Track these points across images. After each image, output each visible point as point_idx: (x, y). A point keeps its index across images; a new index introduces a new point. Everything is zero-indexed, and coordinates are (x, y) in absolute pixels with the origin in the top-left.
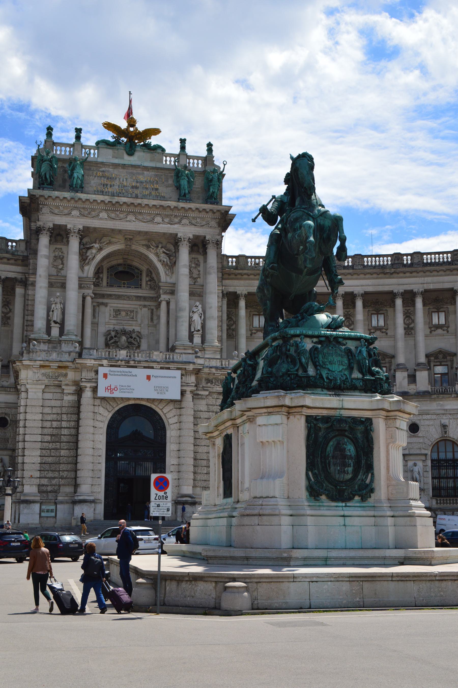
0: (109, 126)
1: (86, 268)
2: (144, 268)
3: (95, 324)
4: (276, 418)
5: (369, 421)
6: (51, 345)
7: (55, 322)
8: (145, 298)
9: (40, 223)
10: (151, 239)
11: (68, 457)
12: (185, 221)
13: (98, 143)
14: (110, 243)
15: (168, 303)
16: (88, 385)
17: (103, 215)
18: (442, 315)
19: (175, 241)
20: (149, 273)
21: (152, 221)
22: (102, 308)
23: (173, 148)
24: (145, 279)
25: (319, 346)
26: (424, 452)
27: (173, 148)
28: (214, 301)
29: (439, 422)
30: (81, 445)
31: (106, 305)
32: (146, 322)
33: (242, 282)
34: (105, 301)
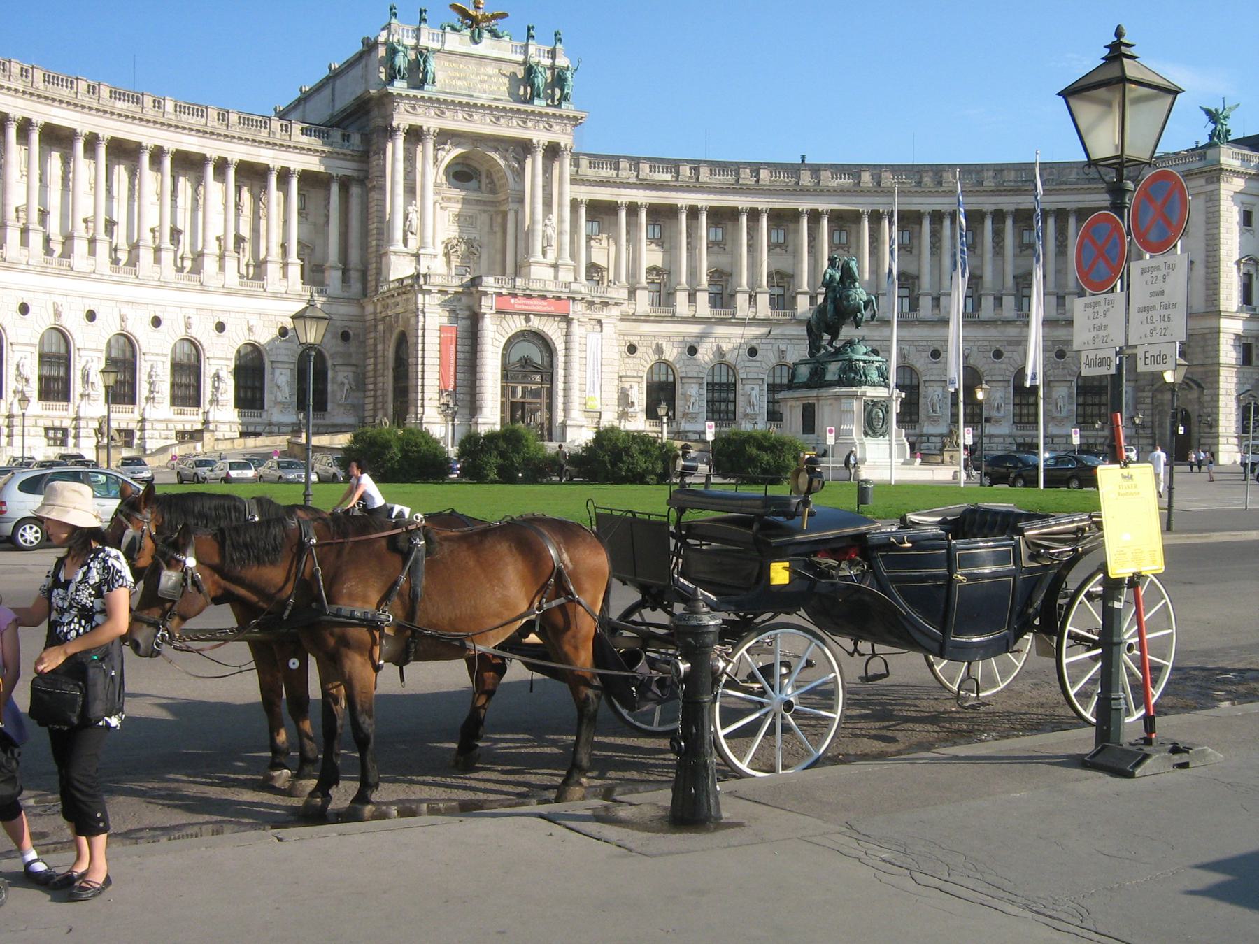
0: (455, 7)
2: (483, 169)
8: (485, 203)
10: (499, 143)
15: (517, 212)
18: (782, 233)
24: (484, 181)
26: (761, 376)
29: (775, 347)
32: (486, 229)
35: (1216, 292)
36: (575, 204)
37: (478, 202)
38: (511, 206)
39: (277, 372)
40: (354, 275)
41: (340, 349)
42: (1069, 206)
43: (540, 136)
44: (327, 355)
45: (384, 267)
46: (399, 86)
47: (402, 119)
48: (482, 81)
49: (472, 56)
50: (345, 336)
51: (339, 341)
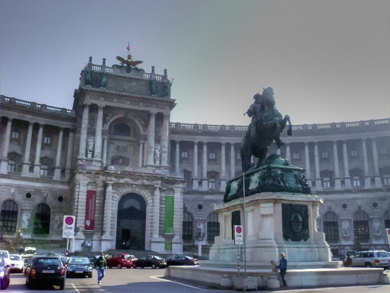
0: (119, 58)
1: (105, 125)
3: (108, 153)
4: (271, 205)
5: (306, 206)
6: (88, 162)
7: (90, 151)
8: (132, 141)
9: (84, 103)
11: (98, 218)
12: (154, 105)
13: (113, 66)
14: (117, 114)
15: (144, 144)
16: (110, 183)
17: (115, 100)
20: (134, 129)
21: (138, 105)
22: (111, 145)
23: (148, 70)
25: (283, 173)
27: (148, 70)
28: (166, 144)
30: (105, 212)
31: (113, 143)
33: (179, 136)
34: (114, 141)
36: (173, 143)
38: (141, 141)
40: (67, 172)
41: (57, 205)
44: (51, 207)
50: (60, 199)
51: (57, 201)
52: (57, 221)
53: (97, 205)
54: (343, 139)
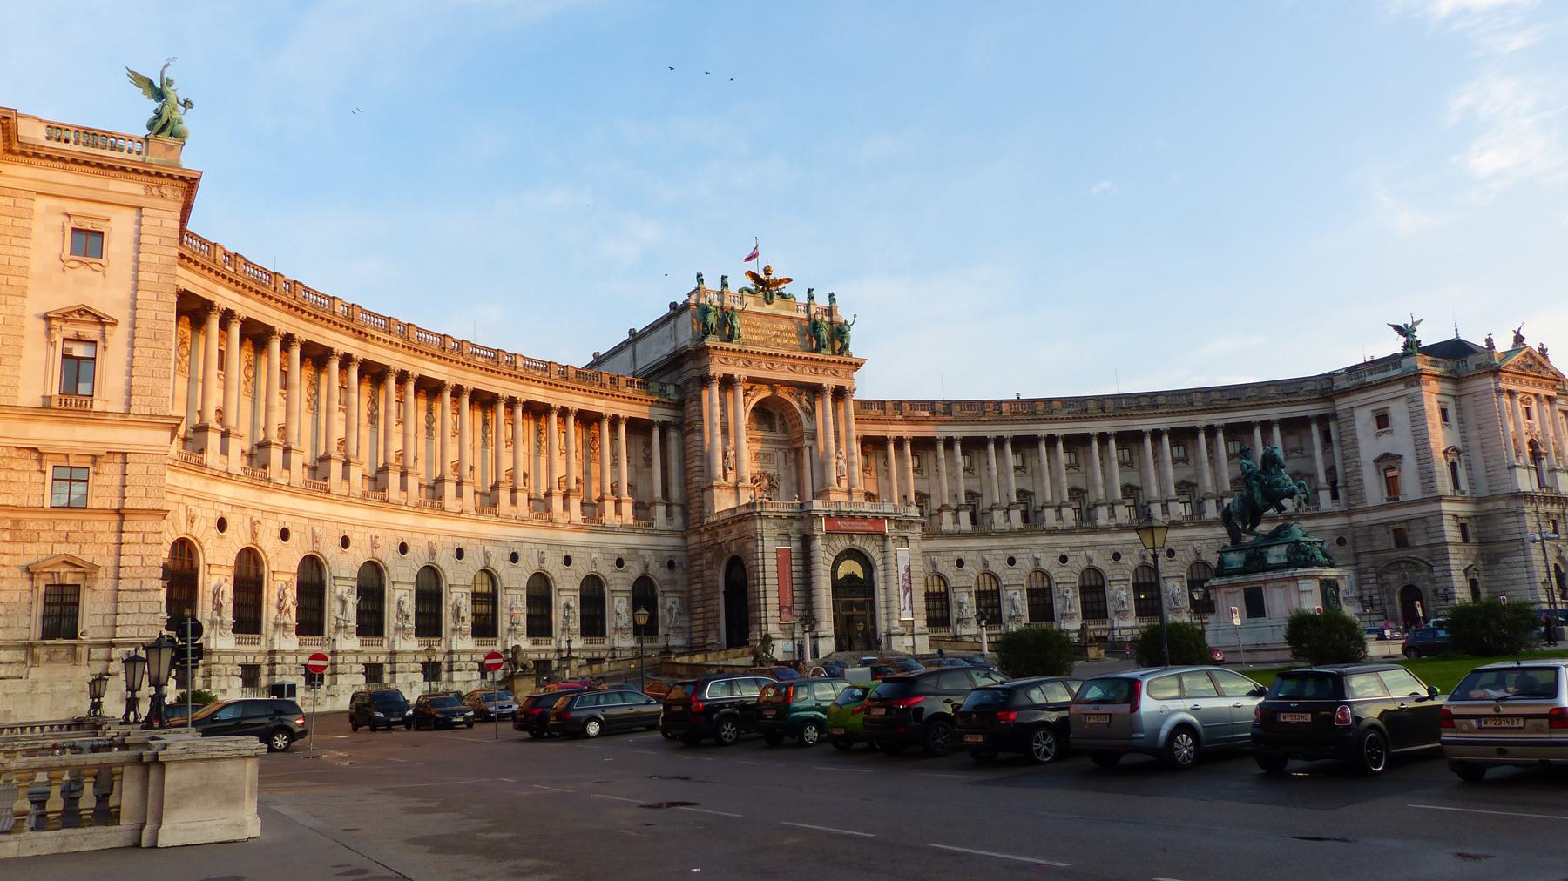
2: (776, 412)
8: (779, 442)
19: (815, 391)
23: (802, 298)
32: (782, 464)
35: (1432, 480)
37: (774, 441)
39: (616, 600)
40: (676, 509)
42: (1272, 418)
43: (829, 382)
45: (707, 504)
46: (712, 341)
47: (717, 369)
48: (776, 336)
49: (766, 315)
50: (671, 565)
52: (671, 609)
53: (795, 575)
54: (1162, 427)
